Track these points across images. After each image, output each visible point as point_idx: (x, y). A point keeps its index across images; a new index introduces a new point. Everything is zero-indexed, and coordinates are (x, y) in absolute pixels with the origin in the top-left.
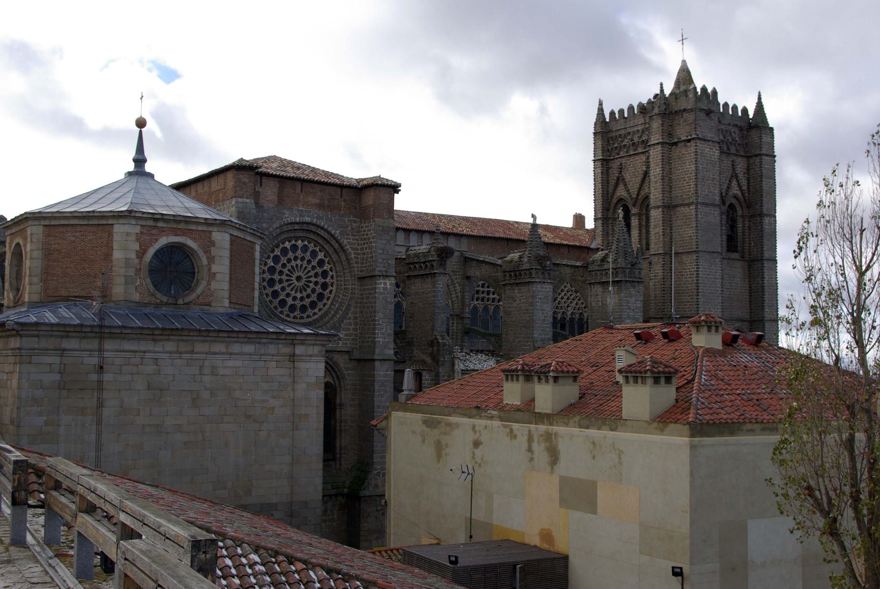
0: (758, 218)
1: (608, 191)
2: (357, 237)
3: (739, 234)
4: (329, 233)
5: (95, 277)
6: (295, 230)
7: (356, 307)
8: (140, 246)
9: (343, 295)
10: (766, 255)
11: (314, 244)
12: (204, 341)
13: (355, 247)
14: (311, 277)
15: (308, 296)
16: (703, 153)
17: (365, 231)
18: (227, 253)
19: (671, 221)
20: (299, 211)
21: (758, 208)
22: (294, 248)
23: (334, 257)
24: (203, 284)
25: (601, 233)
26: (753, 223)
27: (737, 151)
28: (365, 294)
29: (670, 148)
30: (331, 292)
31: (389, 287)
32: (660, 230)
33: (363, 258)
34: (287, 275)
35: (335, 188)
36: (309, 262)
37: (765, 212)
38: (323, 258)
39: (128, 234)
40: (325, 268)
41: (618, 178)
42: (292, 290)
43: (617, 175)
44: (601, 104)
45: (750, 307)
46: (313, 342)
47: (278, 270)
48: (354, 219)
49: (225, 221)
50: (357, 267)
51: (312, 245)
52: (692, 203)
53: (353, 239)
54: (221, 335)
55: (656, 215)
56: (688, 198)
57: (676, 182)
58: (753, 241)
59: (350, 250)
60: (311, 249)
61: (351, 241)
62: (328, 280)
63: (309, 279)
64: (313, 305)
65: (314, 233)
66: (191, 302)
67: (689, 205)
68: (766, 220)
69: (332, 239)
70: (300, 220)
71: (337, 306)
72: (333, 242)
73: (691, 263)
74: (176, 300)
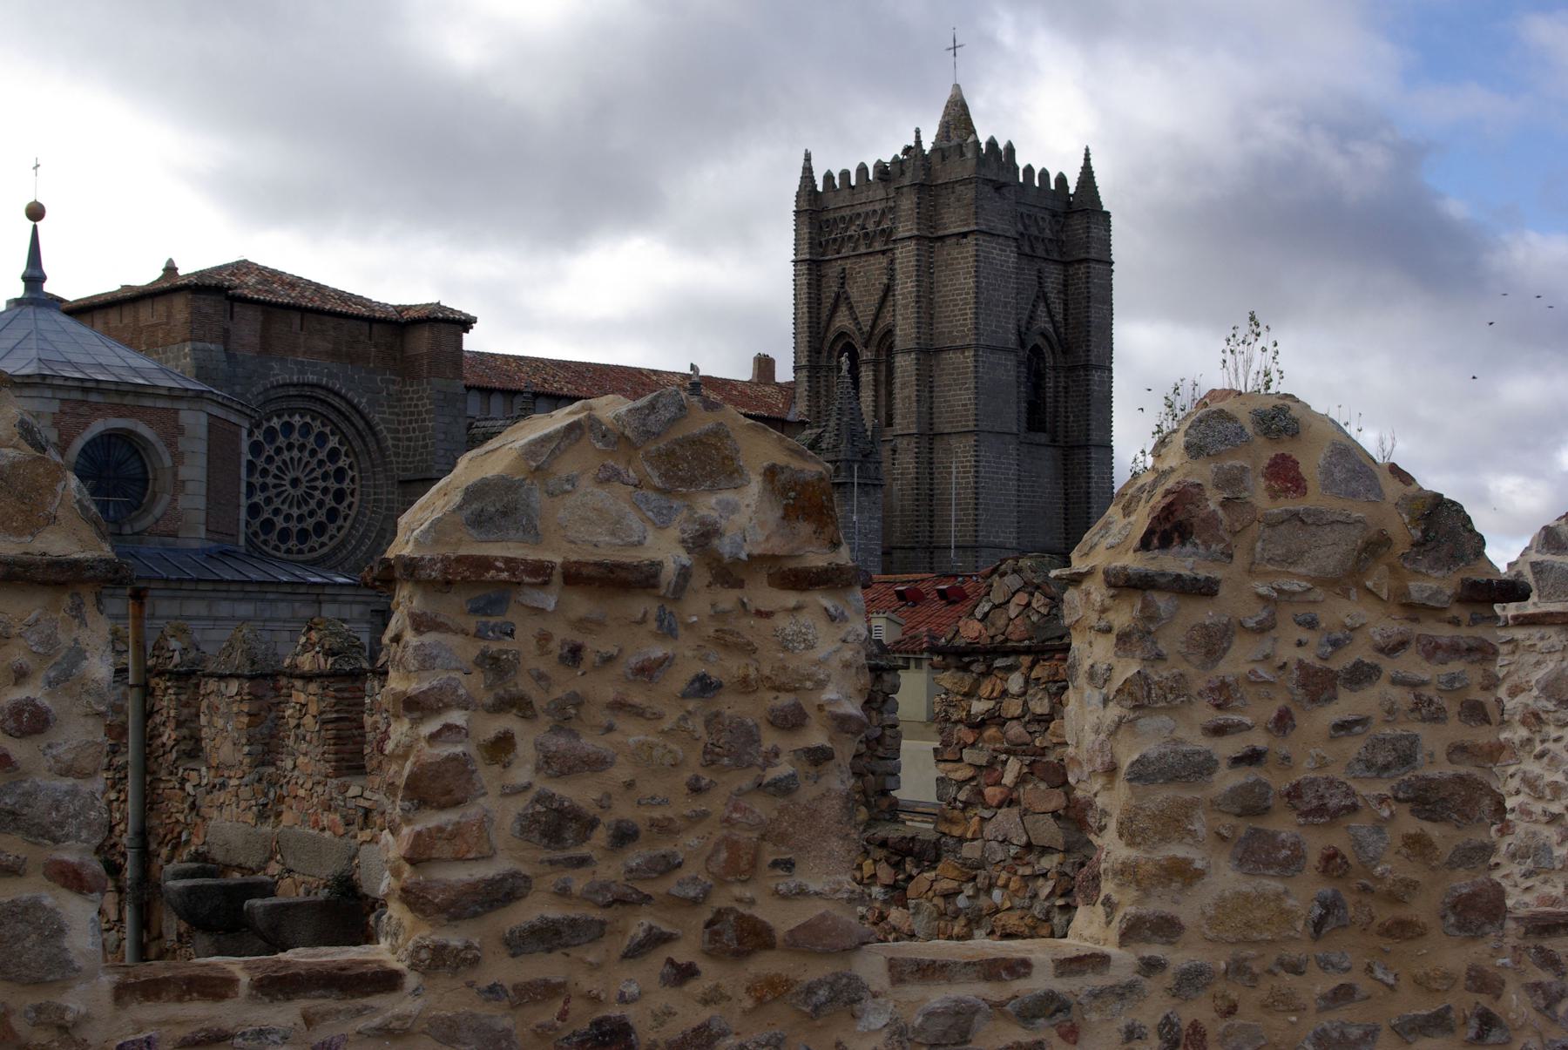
0: (1082, 373)
1: (819, 318)
2: (396, 410)
3: (1048, 400)
4: (349, 402)
6: (289, 396)
9: (373, 512)
10: (1095, 437)
11: (322, 422)
12: (174, 598)
13: (393, 427)
14: (316, 479)
15: (312, 514)
16: (988, 258)
17: (411, 399)
18: (202, 447)
19: (931, 377)
20: (296, 363)
21: (1081, 353)
22: (288, 428)
23: (357, 444)
24: (167, 498)
25: (806, 393)
26: (1074, 381)
27: (1047, 251)
29: (931, 247)
30: (350, 506)
32: (911, 391)
34: (276, 477)
35: (358, 323)
36: (313, 453)
38: (337, 446)
40: (341, 464)
41: (838, 296)
42: (283, 502)
43: (836, 289)
44: (808, 158)
45: (1066, 529)
46: (351, 598)
47: (259, 468)
48: (393, 377)
49: (203, 391)
50: (398, 463)
51: (318, 423)
52: (968, 347)
53: (390, 414)
54: (201, 587)
55: (904, 364)
56: (963, 337)
57: (940, 307)
59: (385, 433)
60: (316, 431)
61: (386, 416)
62: (345, 485)
64: (320, 529)
65: (323, 402)
66: (145, 531)
67: (963, 349)
68: (1096, 376)
69: (353, 412)
70: (298, 378)
71: (361, 530)
72: (356, 419)
74: (120, 529)
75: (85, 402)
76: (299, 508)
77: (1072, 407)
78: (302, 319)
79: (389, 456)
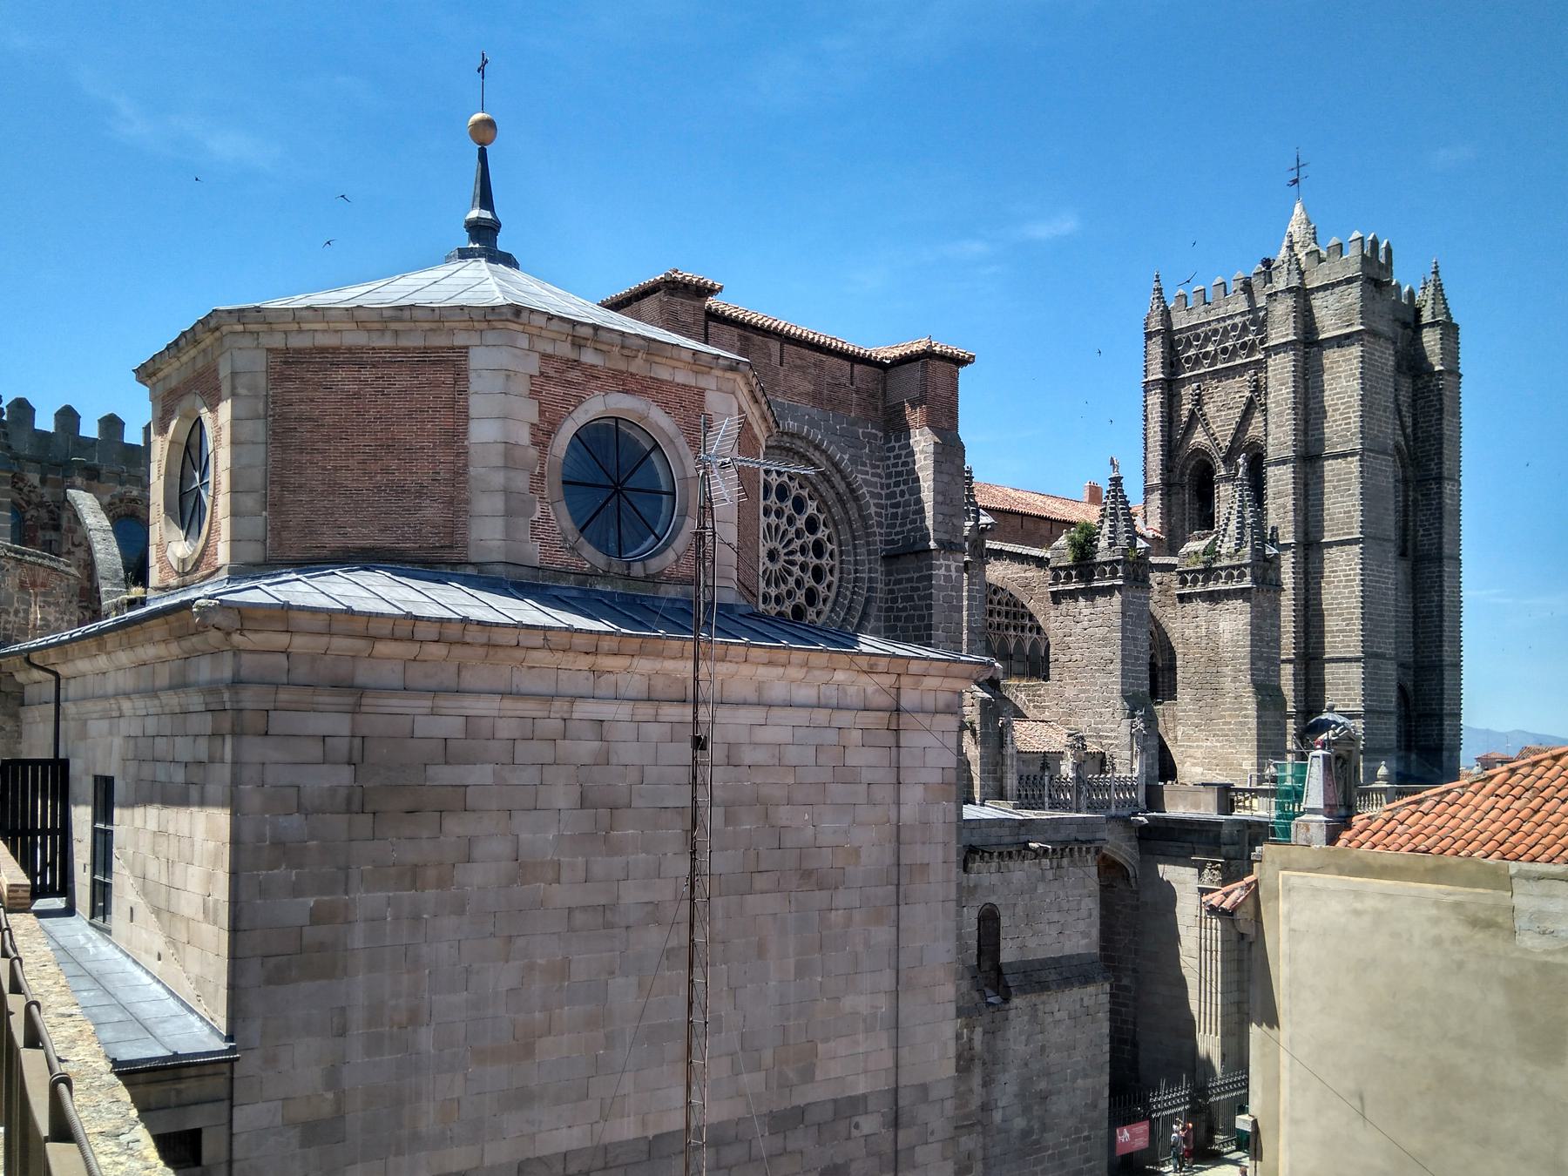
2: (879, 471)
5: (419, 495)
7: (878, 619)
8: (541, 413)
10: (1447, 550)
13: (876, 491)
15: (790, 594)
17: (898, 457)
21: (1432, 466)
26: (1422, 495)
28: (900, 590)
30: (829, 587)
33: (895, 516)
37: (1446, 474)
39: (509, 374)
43: (1190, 406)
48: (874, 431)
49: (738, 362)
50: (881, 534)
52: (1352, 454)
53: (873, 475)
58: (1420, 526)
62: (825, 561)
66: (661, 573)
67: (1344, 455)
68: (1448, 487)
72: (836, 479)
73: (1349, 560)
74: (629, 568)
77: (1422, 521)
79: (872, 526)
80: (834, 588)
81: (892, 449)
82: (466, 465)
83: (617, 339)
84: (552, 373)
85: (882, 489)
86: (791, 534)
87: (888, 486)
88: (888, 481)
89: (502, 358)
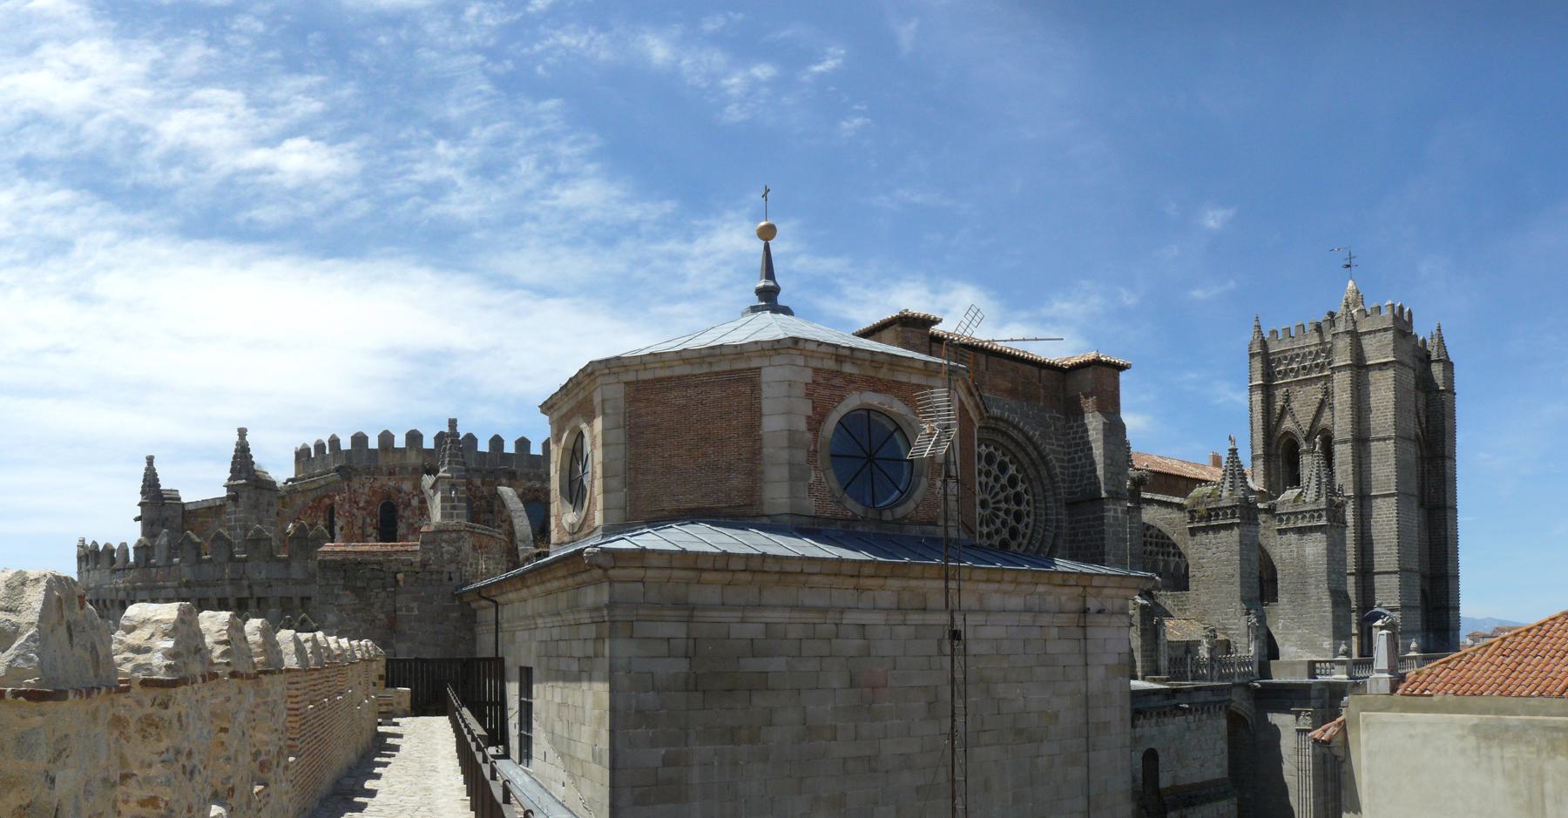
8: (814, 408)
13: (1059, 457)
15: (997, 532)
17: (1077, 432)
23: (1031, 471)
30: (1027, 526)
31: (1120, 515)
33: (1074, 474)
36: (997, 479)
39: (791, 384)
40: (1019, 489)
48: (1058, 415)
59: (1054, 462)
60: (998, 459)
61: (1054, 447)
62: (1023, 507)
63: (997, 505)
65: (1004, 434)
71: (1037, 545)
72: (1030, 449)
75: (838, 373)
76: (987, 527)
78: (987, 361)
79: (1058, 482)
80: (1031, 526)
81: (1072, 427)
82: (761, 448)
83: (867, 356)
84: (821, 381)
85: (1065, 455)
86: (998, 487)
87: (1069, 453)
88: (1070, 450)
89: (785, 373)
